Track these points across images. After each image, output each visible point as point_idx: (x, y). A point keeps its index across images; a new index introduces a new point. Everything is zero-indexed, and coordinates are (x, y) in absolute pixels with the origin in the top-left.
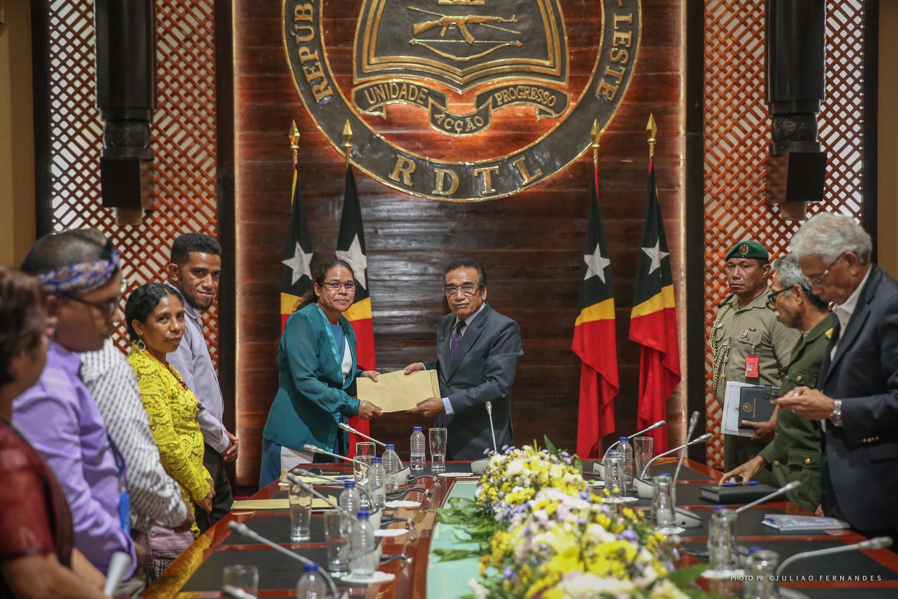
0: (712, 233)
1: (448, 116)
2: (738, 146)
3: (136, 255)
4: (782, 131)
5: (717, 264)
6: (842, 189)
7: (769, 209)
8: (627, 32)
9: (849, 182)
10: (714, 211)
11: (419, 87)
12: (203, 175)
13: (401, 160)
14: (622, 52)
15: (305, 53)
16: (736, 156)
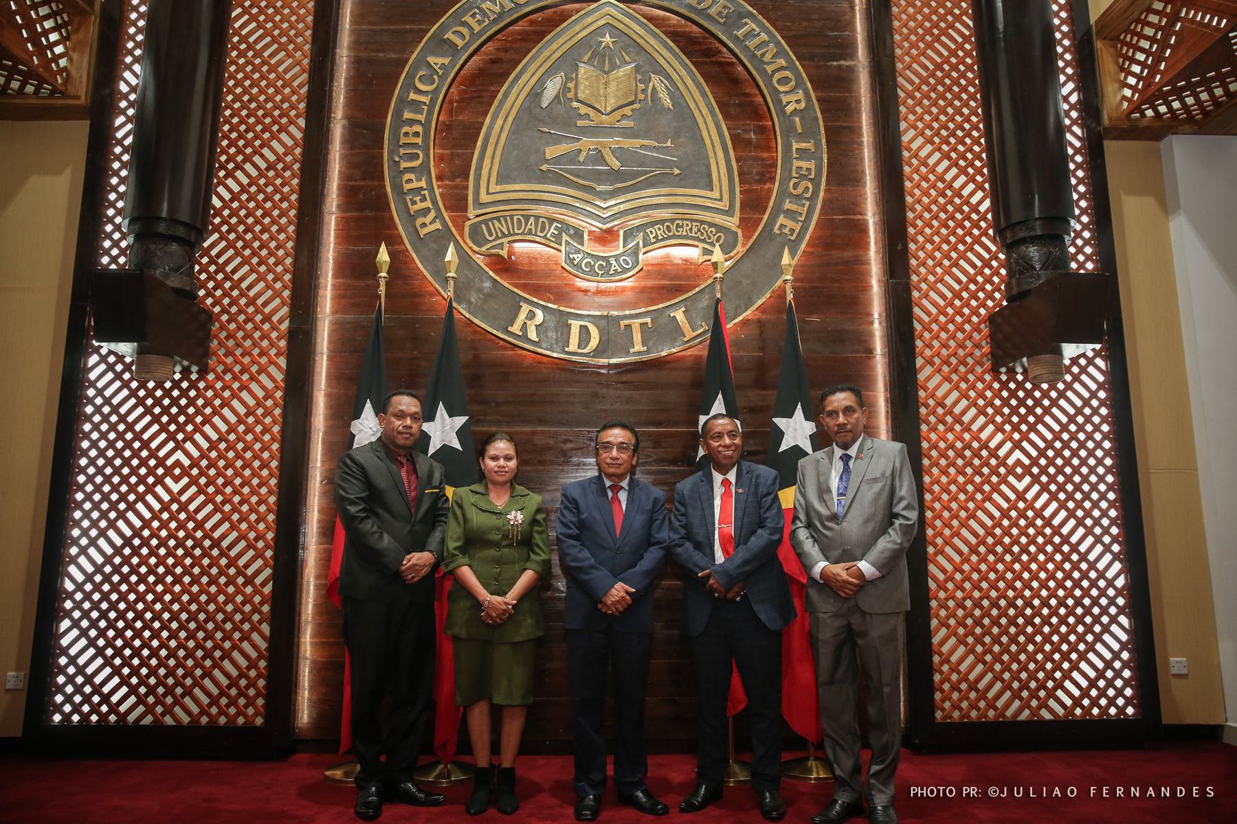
0: (927, 406)
3: (181, 428)
10: (929, 378)
13: (525, 308)
14: (804, 183)
16: (950, 311)
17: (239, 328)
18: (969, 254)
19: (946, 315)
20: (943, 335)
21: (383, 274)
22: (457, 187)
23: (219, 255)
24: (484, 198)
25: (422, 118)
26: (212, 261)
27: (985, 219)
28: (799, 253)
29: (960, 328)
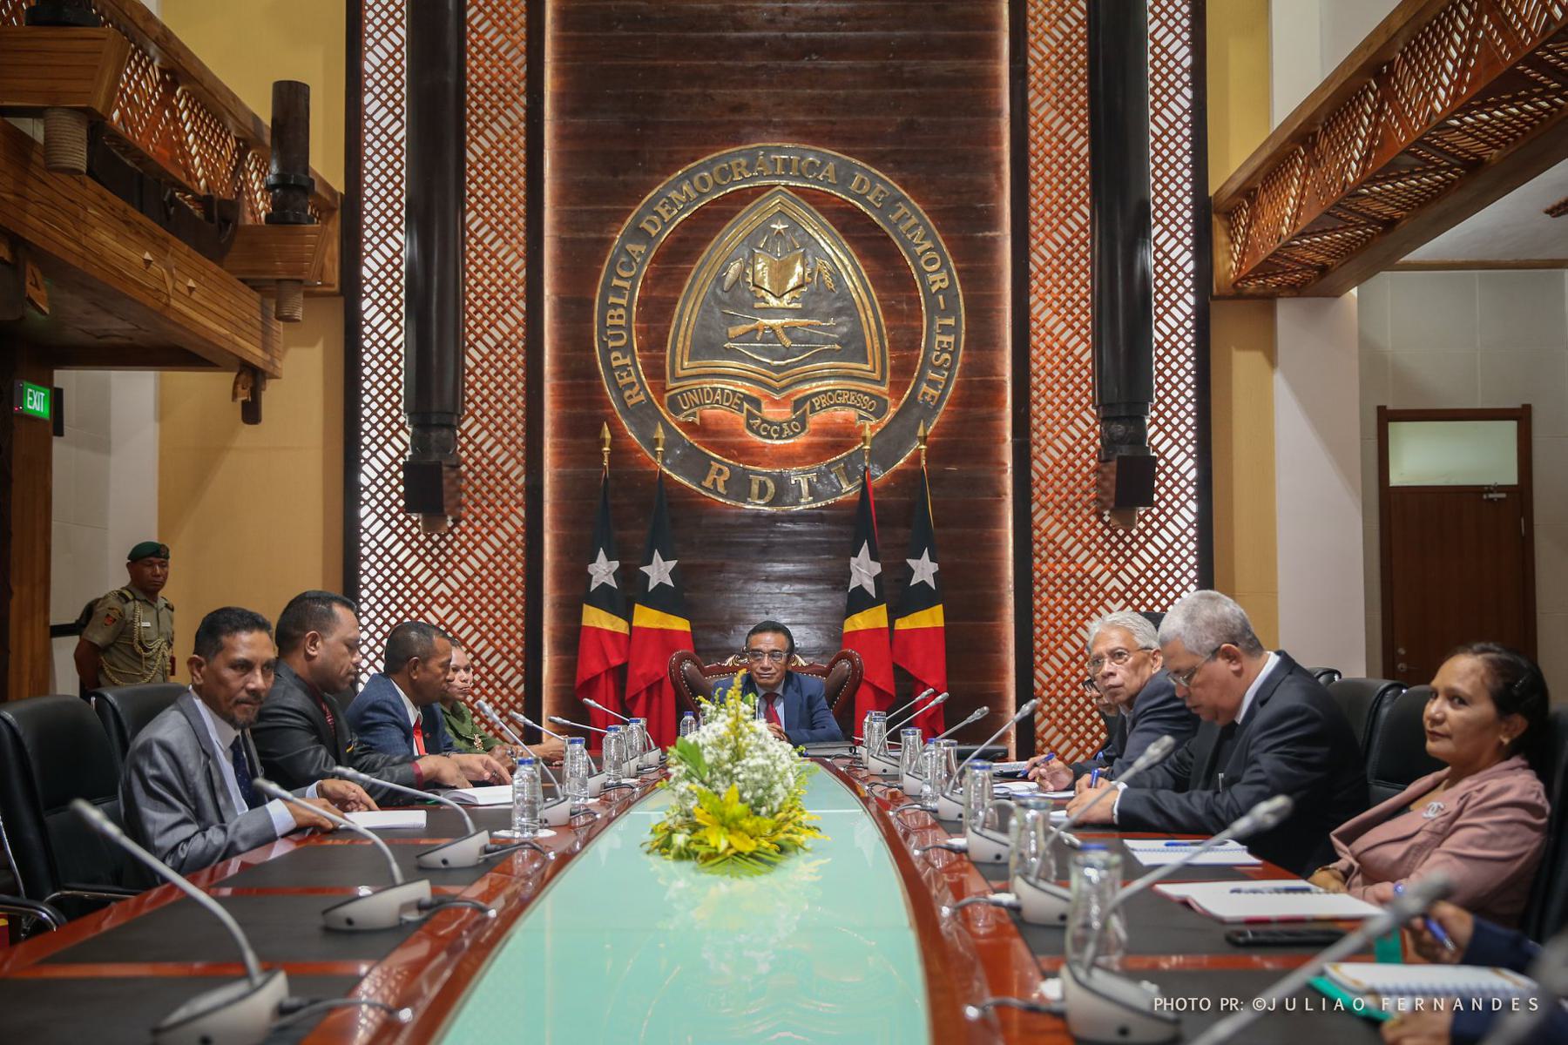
1: (764, 421)
3: (442, 566)
4: (1111, 435)
5: (1045, 576)
6: (1176, 498)
7: (1100, 518)
8: (949, 335)
9: (1183, 491)
10: (1042, 520)
11: (734, 392)
12: (512, 483)
13: (716, 466)
15: (616, 359)
16: (1064, 463)
24: (681, 373)
25: (624, 302)
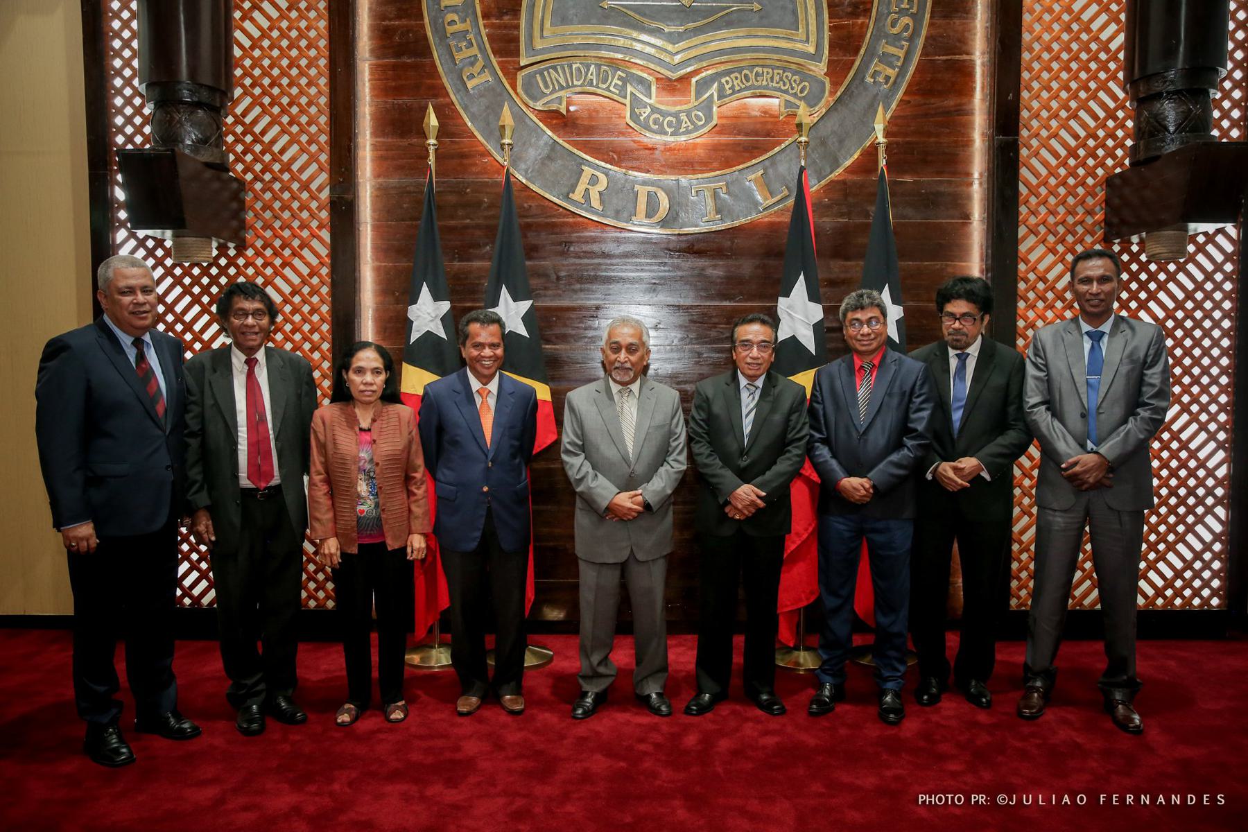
0: (1026, 280)
2: (1067, 157)
10: (1031, 250)
14: (906, 20)
15: (452, 22)
16: (1062, 171)
17: (275, 198)
18: (1092, 104)
19: (1056, 176)
20: (1052, 200)
21: (432, 141)
22: (505, 27)
23: (245, 114)
26: (238, 121)
27: (1115, 59)
28: (894, 106)
29: (1072, 192)
